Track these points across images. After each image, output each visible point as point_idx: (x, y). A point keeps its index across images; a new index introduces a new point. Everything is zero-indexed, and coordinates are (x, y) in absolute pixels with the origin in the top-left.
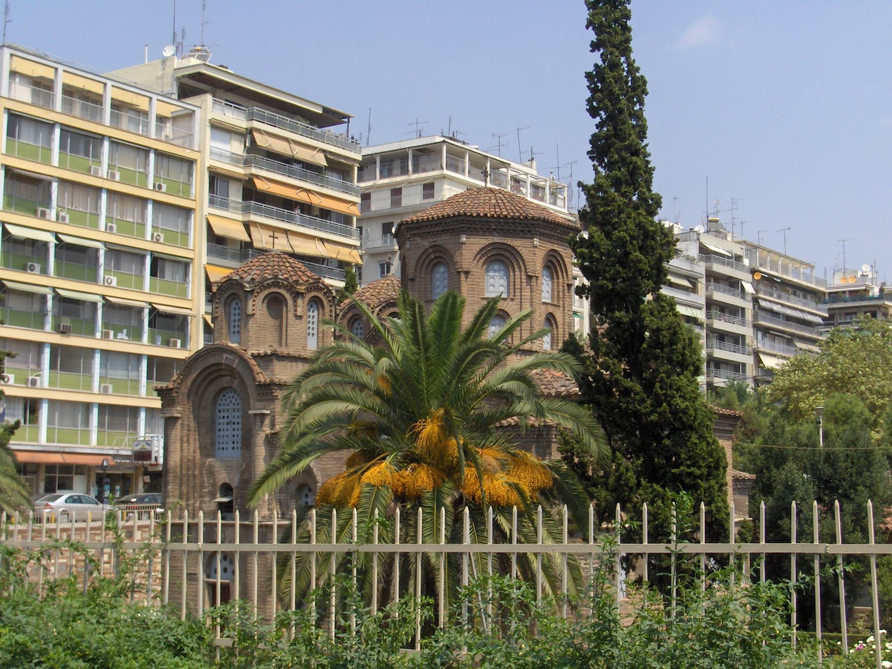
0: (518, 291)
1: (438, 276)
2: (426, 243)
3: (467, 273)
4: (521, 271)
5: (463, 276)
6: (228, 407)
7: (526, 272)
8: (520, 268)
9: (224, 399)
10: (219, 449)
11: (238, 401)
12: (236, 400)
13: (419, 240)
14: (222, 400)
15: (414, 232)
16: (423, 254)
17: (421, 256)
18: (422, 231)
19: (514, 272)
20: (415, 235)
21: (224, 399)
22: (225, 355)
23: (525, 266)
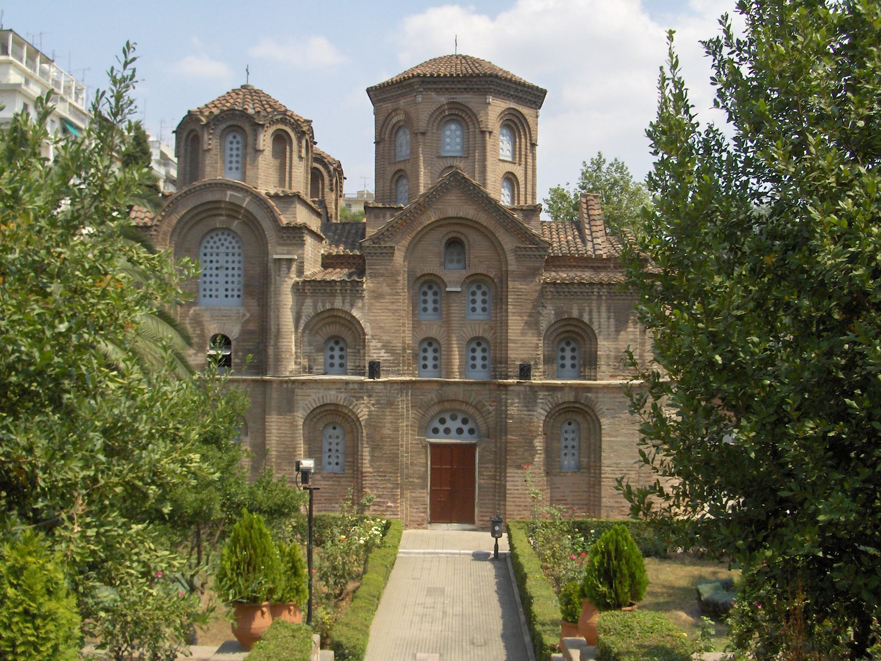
0: (523, 157)
1: (448, 133)
2: (443, 99)
3: (490, 133)
4: (526, 139)
5: (487, 135)
6: (217, 251)
7: (531, 140)
8: (525, 135)
9: (212, 241)
10: (205, 296)
11: (234, 244)
12: (230, 243)
13: (433, 95)
14: (208, 242)
15: (429, 86)
16: (437, 109)
17: (435, 111)
18: (441, 86)
19: (520, 139)
20: (429, 89)
21: (212, 241)
22: (229, 193)
23: (530, 134)
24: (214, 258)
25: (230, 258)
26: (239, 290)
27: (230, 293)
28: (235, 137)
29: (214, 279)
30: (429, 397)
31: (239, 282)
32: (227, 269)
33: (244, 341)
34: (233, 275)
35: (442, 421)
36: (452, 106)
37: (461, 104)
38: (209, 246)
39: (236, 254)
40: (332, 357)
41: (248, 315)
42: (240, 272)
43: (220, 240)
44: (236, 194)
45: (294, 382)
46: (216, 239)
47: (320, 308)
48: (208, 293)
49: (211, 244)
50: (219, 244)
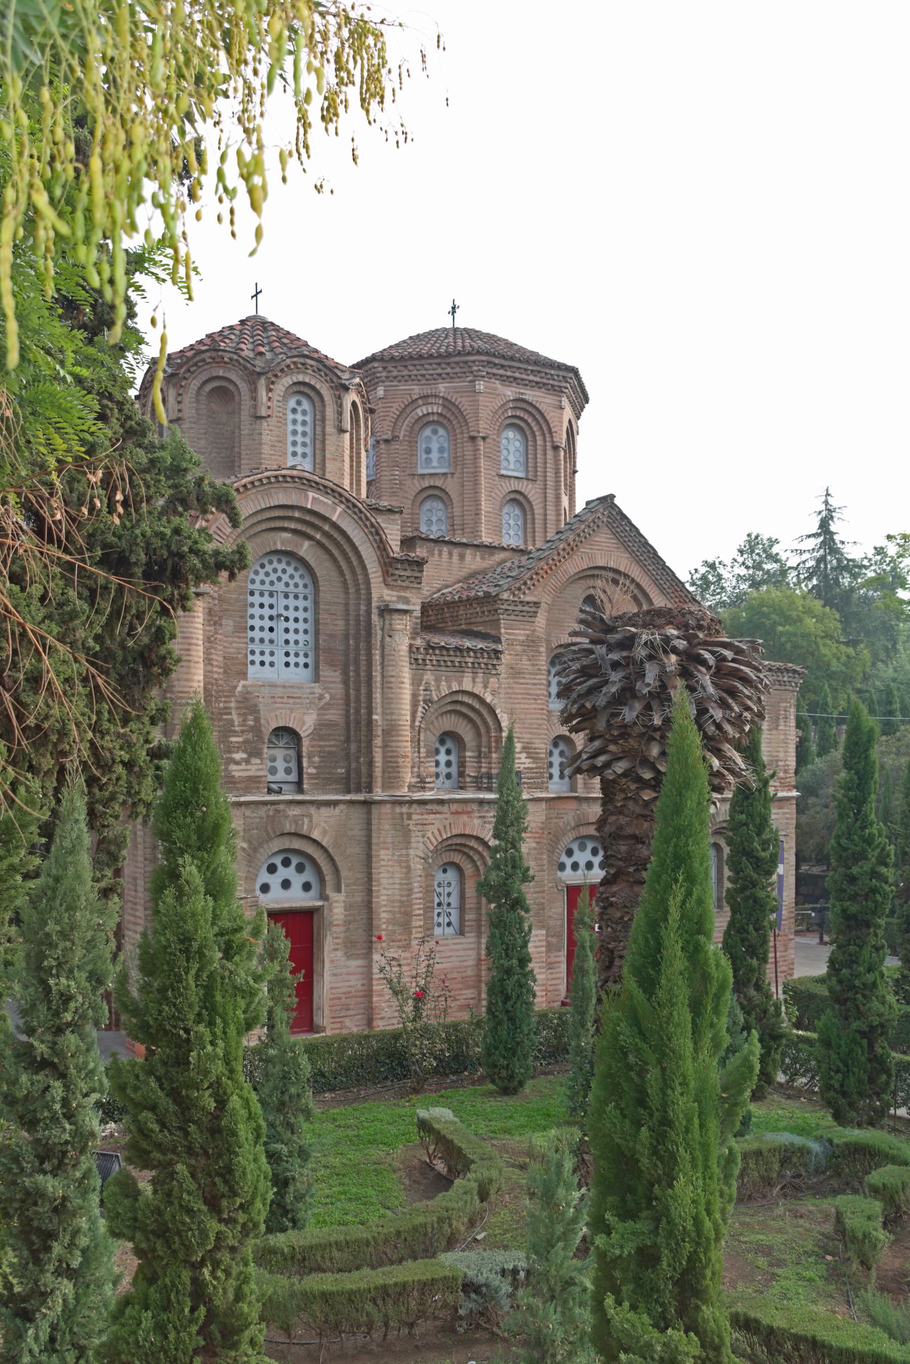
2: (510, 392)
6: (272, 588)
11: (297, 579)
15: (495, 371)
18: (509, 373)
21: (262, 571)
22: (311, 495)
24: (267, 600)
25: (292, 602)
26: (306, 655)
27: (292, 660)
28: (299, 403)
29: (267, 635)
30: (565, 820)
31: (306, 643)
32: (287, 619)
33: (322, 738)
34: (296, 631)
35: (570, 853)
36: (519, 405)
37: (531, 404)
38: (258, 579)
39: (301, 596)
40: (437, 764)
41: (327, 696)
42: (306, 626)
43: (275, 571)
44: (322, 498)
45: (412, 802)
46: (290, 570)
47: (445, 691)
48: (257, 658)
49: (262, 576)
50: (273, 577)
